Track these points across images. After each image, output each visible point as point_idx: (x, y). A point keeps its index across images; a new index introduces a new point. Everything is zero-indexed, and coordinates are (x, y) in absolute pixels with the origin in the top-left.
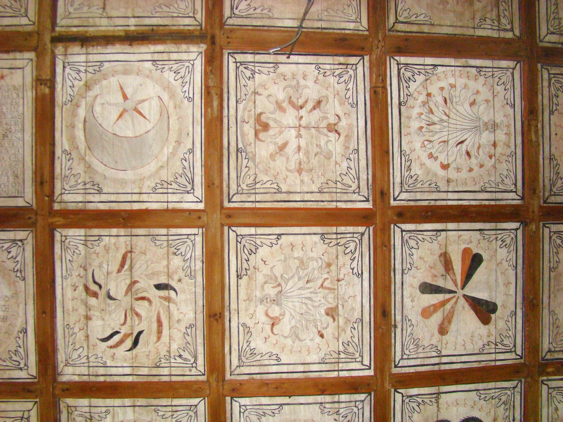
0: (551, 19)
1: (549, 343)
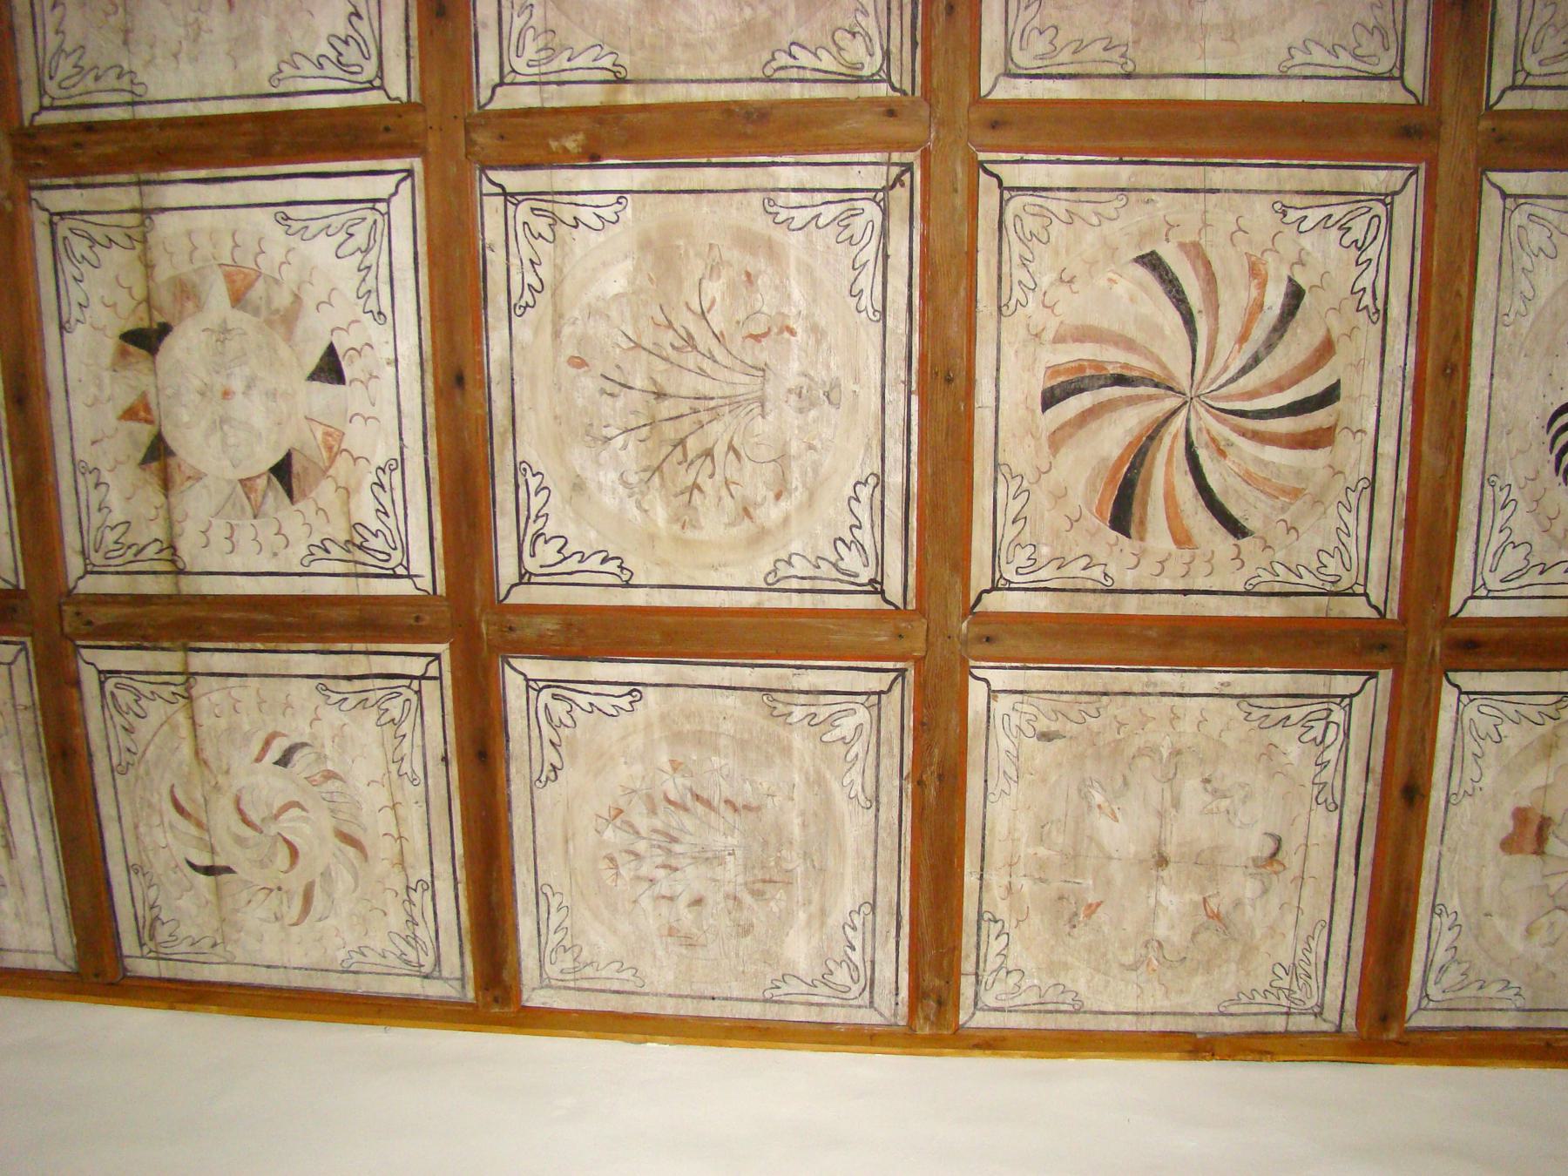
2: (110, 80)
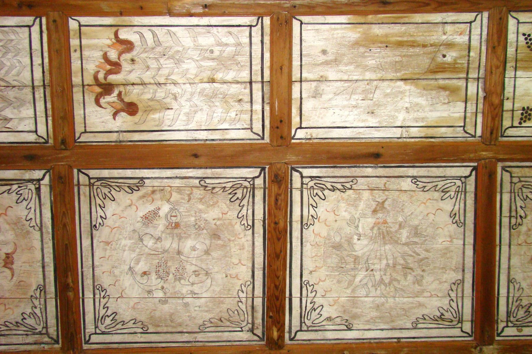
1: (242, 331)
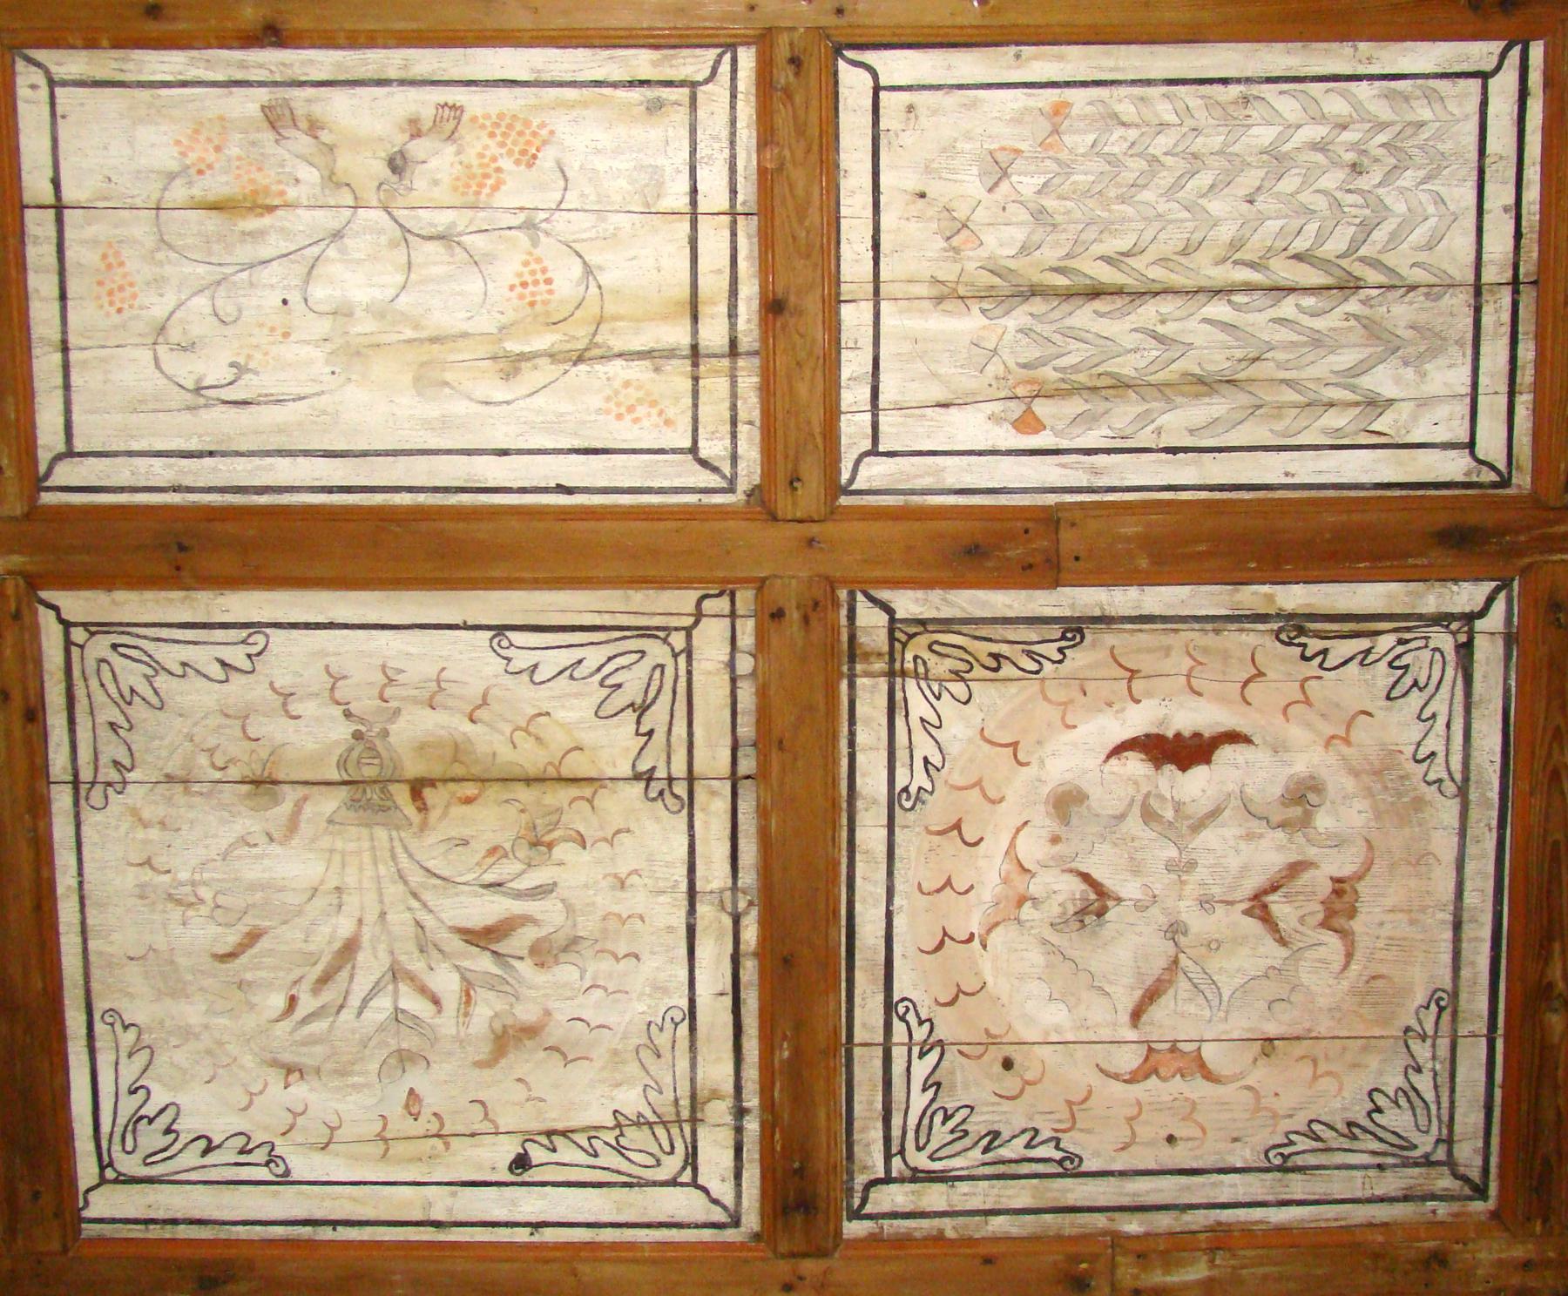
0: (624, 1166)
2: (112, 749)
